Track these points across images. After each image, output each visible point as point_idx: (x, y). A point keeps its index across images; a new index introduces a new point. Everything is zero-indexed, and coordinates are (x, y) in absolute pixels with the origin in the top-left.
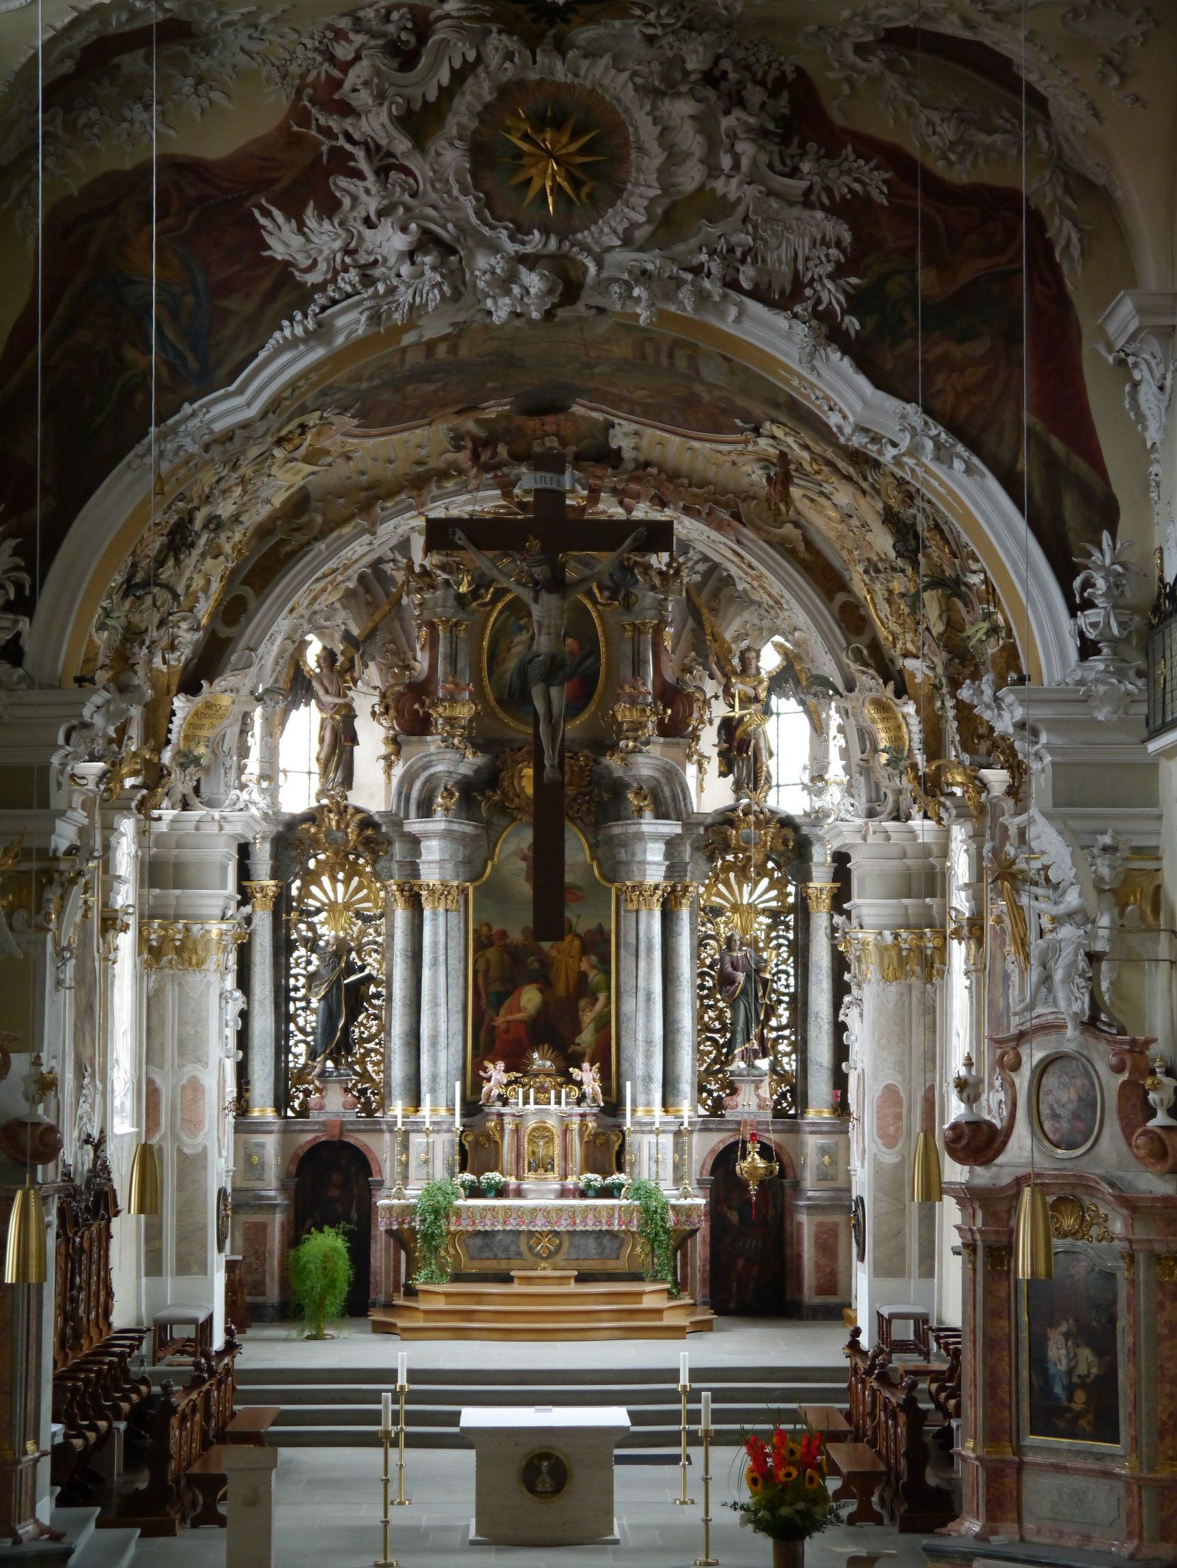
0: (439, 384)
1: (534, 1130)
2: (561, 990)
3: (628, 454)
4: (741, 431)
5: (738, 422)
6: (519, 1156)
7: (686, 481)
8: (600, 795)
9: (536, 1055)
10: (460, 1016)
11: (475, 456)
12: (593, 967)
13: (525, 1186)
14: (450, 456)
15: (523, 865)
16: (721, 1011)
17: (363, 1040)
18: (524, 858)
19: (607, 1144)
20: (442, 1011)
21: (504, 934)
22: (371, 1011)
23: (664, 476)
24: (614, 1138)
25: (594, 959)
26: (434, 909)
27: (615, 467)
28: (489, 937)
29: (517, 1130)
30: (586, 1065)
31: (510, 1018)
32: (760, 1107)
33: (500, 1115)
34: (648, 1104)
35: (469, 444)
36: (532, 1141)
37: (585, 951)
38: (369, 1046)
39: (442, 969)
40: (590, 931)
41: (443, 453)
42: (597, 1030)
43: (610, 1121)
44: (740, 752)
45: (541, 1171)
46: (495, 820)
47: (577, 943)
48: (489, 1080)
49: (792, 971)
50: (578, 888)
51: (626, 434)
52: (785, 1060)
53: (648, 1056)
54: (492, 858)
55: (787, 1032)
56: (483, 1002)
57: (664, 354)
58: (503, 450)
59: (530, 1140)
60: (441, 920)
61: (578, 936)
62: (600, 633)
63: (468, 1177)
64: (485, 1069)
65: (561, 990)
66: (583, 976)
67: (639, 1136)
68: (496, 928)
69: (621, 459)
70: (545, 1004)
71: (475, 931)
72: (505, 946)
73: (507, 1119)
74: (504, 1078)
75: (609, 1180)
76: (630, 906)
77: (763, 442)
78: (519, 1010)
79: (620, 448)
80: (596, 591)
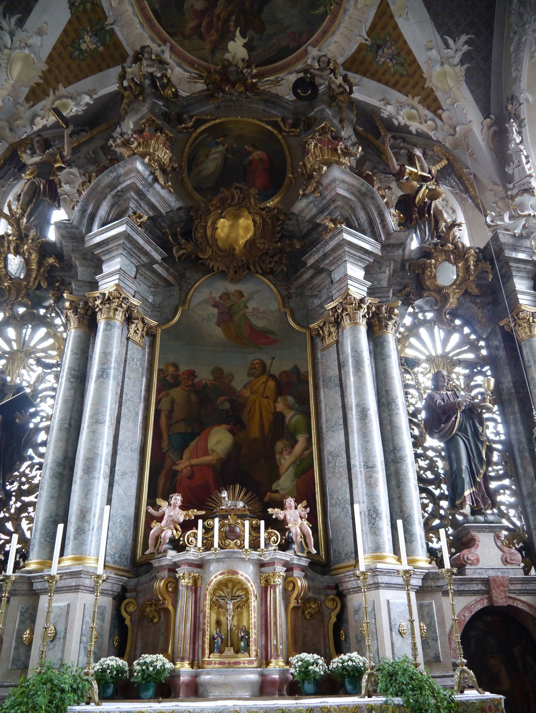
1: (221, 585)
2: (255, 432)
6: (197, 629)
8: (291, 245)
9: (225, 494)
10: (136, 456)
12: (291, 408)
13: (205, 678)
15: (215, 311)
16: (431, 459)
17: (20, 493)
18: (216, 305)
19: (320, 614)
20: (107, 431)
21: (192, 374)
22: (37, 460)
24: (330, 605)
25: (290, 399)
26: (109, 319)
28: (176, 377)
29: (195, 588)
30: (290, 501)
31: (194, 461)
32: (505, 561)
33: (173, 568)
34: (377, 548)
36: (216, 605)
37: (280, 391)
38: (26, 499)
39: (112, 386)
40: (285, 372)
42: (297, 475)
43: (324, 580)
44: (421, 215)
45: (230, 651)
46: (188, 274)
47: (271, 384)
48: (160, 519)
49: (499, 419)
50: (272, 333)
52: (512, 512)
53: (371, 484)
54: (184, 303)
55: (506, 482)
56: (165, 444)
59: (215, 604)
60: (117, 332)
61: (272, 376)
62: (286, 148)
63: (113, 661)
64: (157, 507)
65: (255, 432)
66: (279, 417)
67: (371, 594)
68: (183, 368)
70: (236, 446)
71: (160, 370)
72: (193, 385)
73: (181, 572)
74: (181, 516)
75: (336, 662)
76: (328, 341)
78: (206, 453)
80: (282, 124)
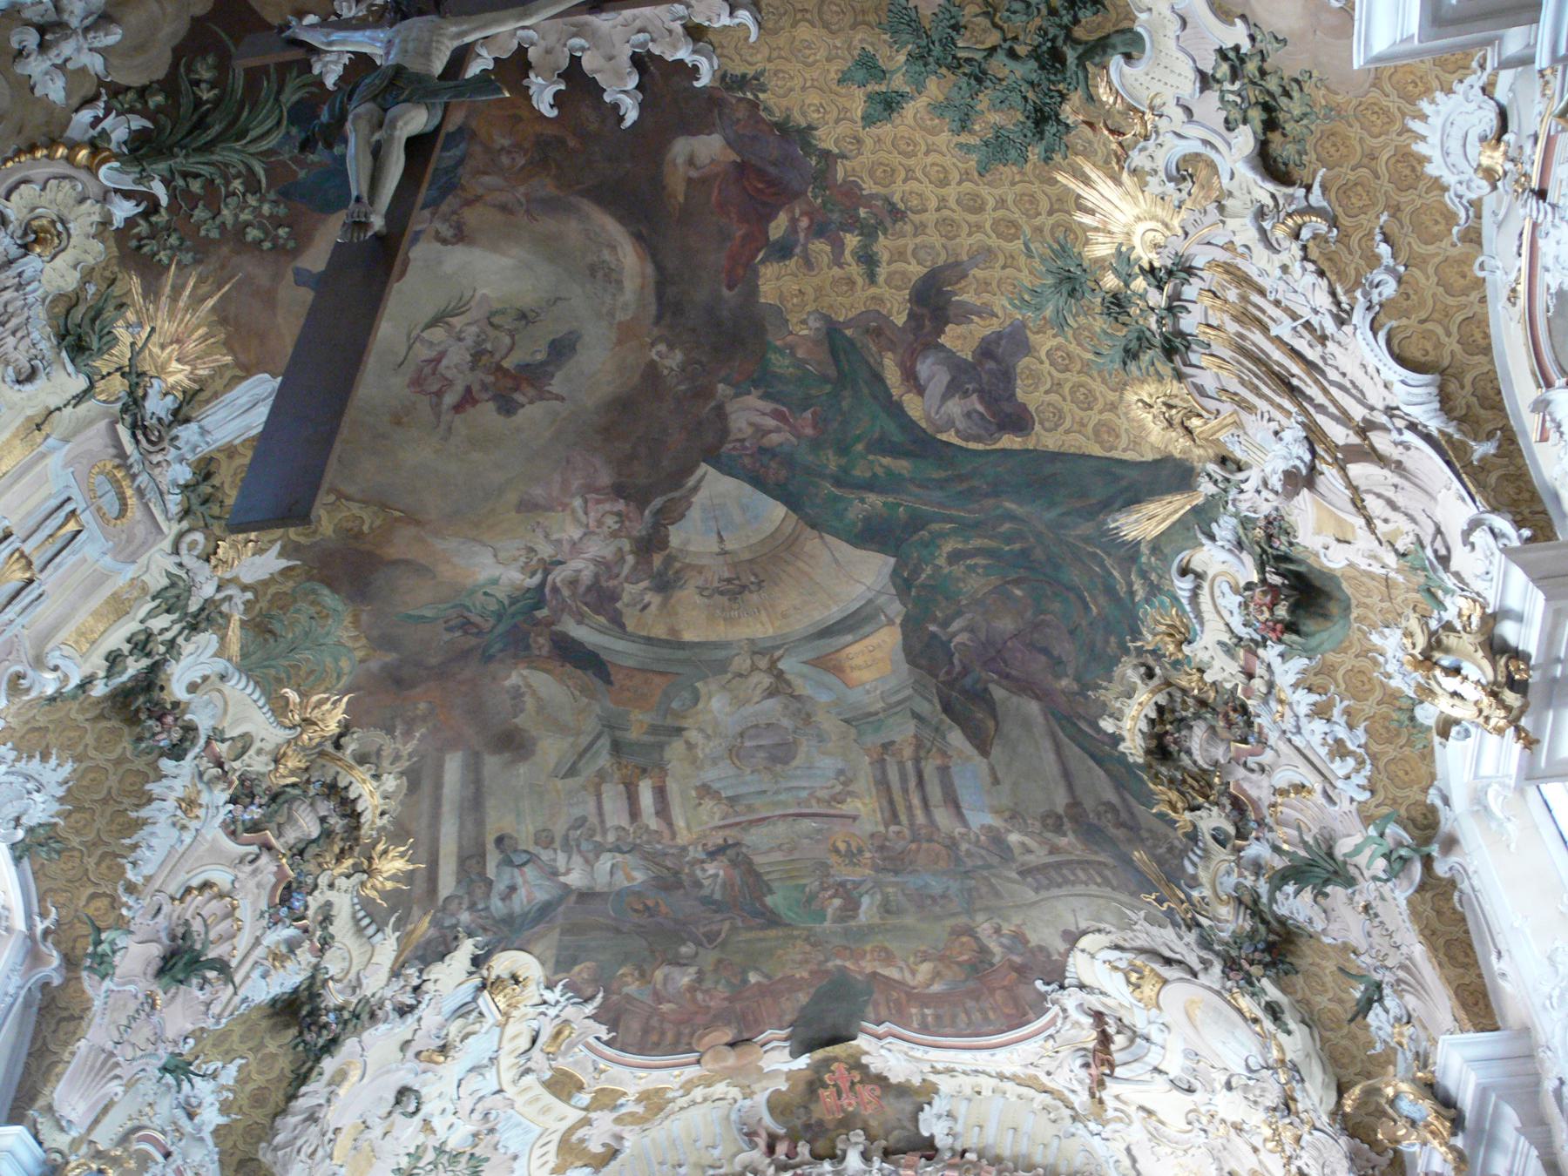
0: (692, 970)
3: (942, 1141)
4: (1043, 997)
5: (1039, 984)
7: (1011, 1165)
11: (771, 1150)
14: (745, 1157)
23: (984, 1162)
27: (929, 1158)
35: (764, 1135)
41: (735, 1155)
51: (939, 1117)
57: (912, 783)
58: (804, 1150)
69: (937, 1150)
77: (1071, 999)
79: (932, 1137)
